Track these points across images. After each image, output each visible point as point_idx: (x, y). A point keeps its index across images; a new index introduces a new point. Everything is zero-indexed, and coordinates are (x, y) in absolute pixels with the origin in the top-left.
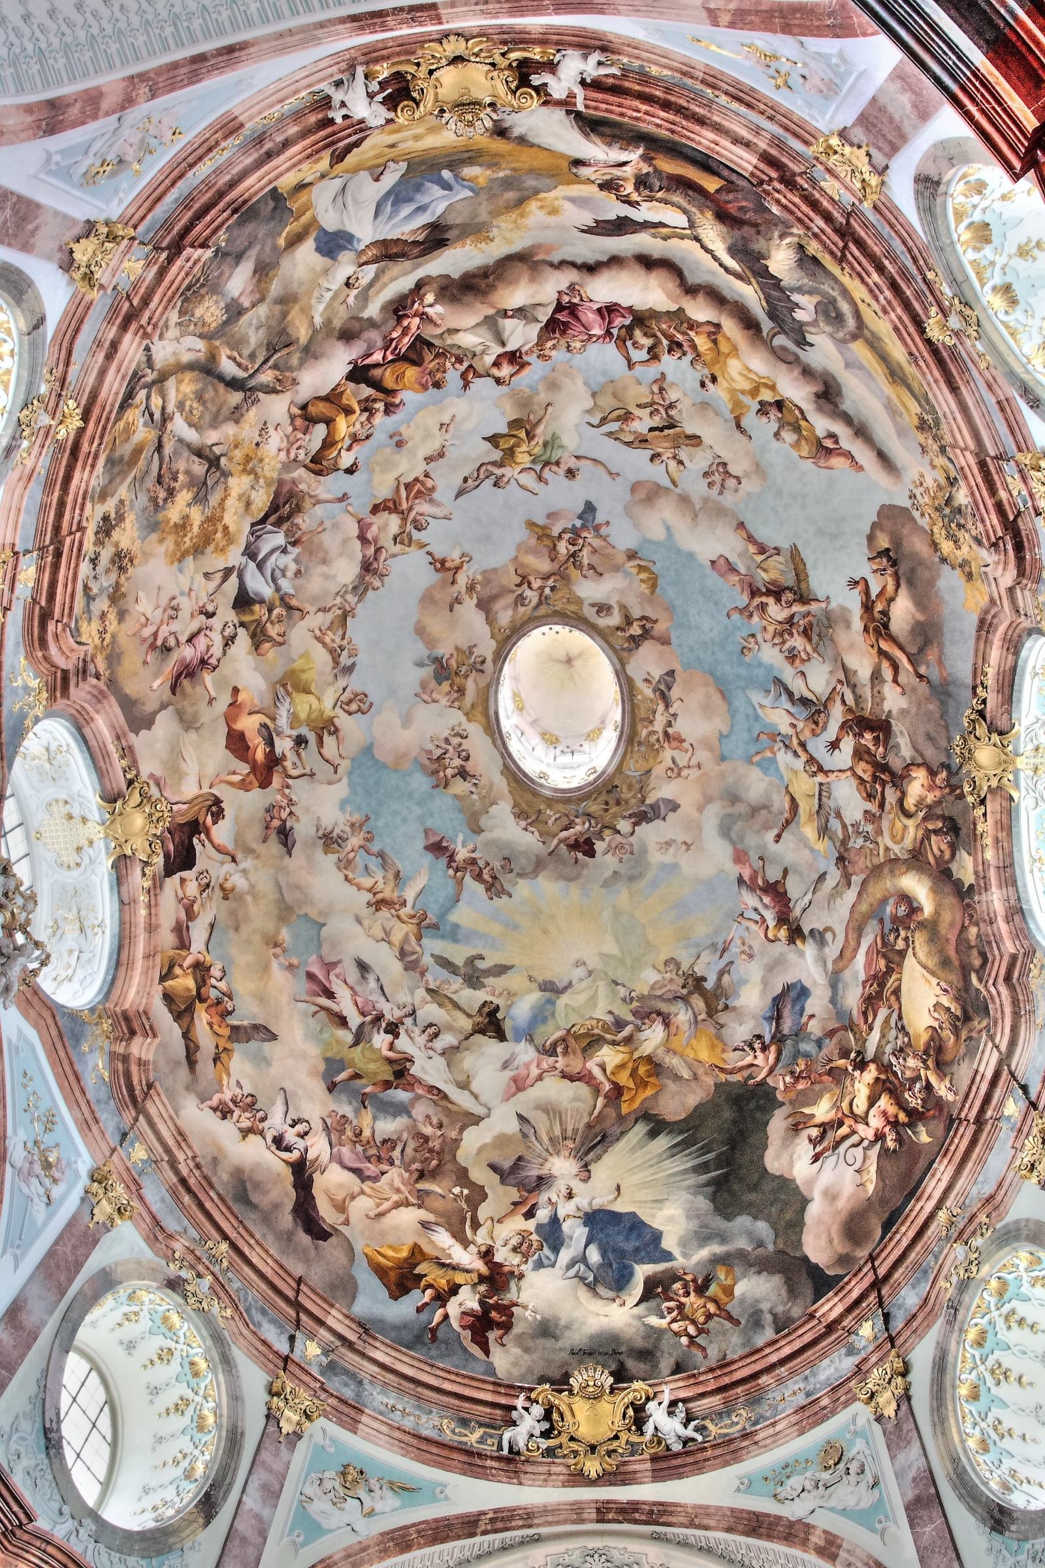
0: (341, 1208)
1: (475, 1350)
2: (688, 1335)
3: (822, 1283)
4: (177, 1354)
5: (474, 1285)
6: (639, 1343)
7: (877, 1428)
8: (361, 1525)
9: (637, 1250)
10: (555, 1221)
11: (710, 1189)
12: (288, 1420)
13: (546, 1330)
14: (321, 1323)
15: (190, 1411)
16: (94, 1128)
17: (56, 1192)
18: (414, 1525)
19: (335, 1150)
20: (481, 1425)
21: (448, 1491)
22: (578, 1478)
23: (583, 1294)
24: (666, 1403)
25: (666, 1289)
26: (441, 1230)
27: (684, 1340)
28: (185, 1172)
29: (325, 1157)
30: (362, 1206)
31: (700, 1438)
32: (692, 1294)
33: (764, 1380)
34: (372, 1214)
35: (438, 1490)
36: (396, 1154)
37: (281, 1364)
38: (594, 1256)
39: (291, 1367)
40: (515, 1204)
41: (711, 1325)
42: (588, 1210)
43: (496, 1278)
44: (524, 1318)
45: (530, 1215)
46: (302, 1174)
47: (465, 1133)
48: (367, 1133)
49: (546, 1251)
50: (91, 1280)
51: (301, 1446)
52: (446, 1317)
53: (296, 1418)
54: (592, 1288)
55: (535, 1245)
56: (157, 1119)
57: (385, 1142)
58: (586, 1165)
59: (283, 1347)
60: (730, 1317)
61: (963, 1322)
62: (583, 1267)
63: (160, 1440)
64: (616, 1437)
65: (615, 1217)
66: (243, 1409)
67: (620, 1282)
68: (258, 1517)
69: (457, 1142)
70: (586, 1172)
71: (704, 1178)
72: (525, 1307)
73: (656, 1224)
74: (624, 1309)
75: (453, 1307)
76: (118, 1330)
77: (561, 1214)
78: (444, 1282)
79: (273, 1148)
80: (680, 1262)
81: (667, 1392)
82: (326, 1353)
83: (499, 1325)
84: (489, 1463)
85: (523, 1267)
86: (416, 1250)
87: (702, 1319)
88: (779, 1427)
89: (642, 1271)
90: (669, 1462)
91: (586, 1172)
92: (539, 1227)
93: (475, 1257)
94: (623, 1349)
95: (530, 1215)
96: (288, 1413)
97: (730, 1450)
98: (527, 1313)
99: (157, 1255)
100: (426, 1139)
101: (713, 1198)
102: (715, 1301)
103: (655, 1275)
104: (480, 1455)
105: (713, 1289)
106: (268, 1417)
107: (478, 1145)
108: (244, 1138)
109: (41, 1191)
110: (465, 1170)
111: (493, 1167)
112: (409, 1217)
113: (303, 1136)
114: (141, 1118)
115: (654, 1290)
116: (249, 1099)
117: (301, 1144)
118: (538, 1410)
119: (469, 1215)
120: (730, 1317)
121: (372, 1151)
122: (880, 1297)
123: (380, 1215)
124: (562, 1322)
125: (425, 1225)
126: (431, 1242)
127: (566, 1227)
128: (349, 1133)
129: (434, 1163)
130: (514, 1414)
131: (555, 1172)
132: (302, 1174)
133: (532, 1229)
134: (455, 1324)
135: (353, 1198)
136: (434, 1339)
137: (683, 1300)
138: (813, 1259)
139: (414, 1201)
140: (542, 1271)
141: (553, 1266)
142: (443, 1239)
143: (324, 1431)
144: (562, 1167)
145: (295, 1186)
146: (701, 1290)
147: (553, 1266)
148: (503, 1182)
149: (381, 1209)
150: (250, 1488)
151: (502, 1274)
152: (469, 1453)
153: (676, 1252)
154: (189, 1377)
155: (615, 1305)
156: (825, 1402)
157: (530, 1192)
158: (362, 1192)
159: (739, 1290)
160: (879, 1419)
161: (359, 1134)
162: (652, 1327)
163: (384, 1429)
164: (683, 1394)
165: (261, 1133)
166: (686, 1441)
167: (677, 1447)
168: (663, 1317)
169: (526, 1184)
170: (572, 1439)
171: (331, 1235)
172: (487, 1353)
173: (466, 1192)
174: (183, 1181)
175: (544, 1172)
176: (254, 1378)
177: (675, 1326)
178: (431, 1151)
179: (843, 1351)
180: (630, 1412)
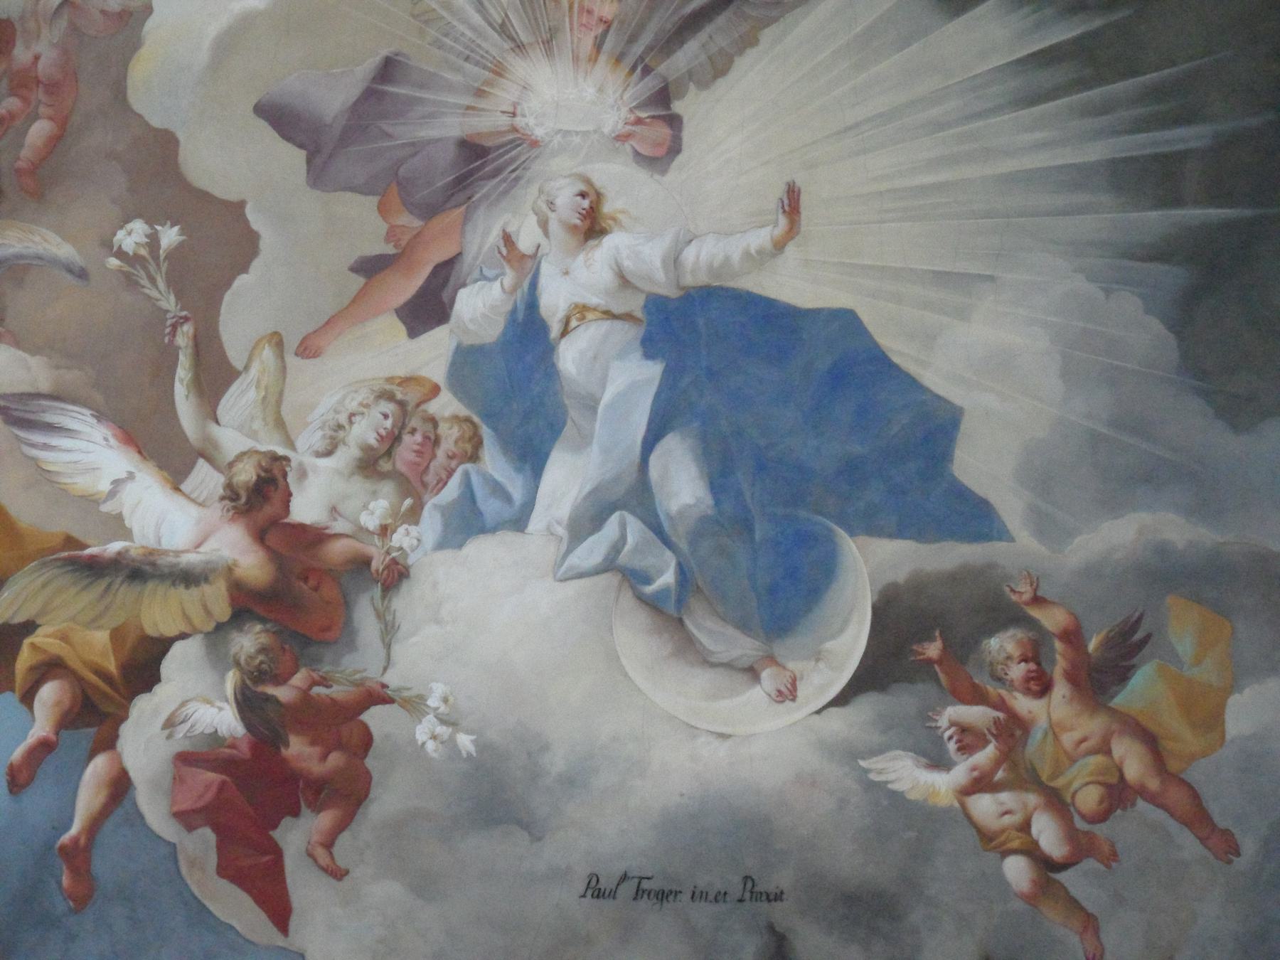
1: (235, 908)
2: (1032, 851)
6: (848, 862)
9: (852, 471)
10: (529, 333)
11: (1172, 277)
13: (497, 794)
23: (635, 641)
25: (962, 649)
26: (79, 420)
27: (1017, 870)
32: (1061, 689)
38: (682, 484)
40: (371, 268)
41: (1122, 830)
42: (663, 285)
43: (301, 594)
44: (415, 744)
45: (427, 310)
49: (494, 463)
52: (120, 786)
54: (668, 614)
55: (450, 435)
58: (663, 97)
60: (1197, 817)
62: (635, 530)
65: (773, 324)
67: (782, 601)
70: (660, 128)
71: (1155, 221)
72: (415, 706)
73: (934, 379)
75: (144, 742)
77: (555, 298)
78: (101, 637)
80: (1020, 548)
83: (319, 792)
85: (402, 538)
87: (1089, 798)
89: (869, 565)
91: (660, 128)
92: (467, 360)
93: (216, 512)
94: (783, 879)
95: (427, 310)
101: (1183, 315)
102: (1150, 740)
103: (919, 584)
105: (1143, 688)
107: (213, 30)
110: (167, 142)
111: (282, 118)
115: (912, 648)
119: (183, 338)
120: (1197, 817)
124: (556, 762)
126: (43, 477)
127: (570, 357)
129: (39, 131)
131: (535, 123)
133: (437, 372)
134: (153, 808)
136: (82, 897)
137: (1023, 704)
141: (519, 523)
142: (91, 455)
144: (566, 101)
146: (1099, 678)
147: (519, 523)
151: (317, 574)
153: (1011, 507)
155: (757, 695)
157: (429, 211)
159: (1244, 713)
162: (897, 798)
168: (939, 762)
169: (415, 172)
172: (279, 911)
173: (170, 236)
175: (488, 122)
177: (985, 806)
178: (23, 82)
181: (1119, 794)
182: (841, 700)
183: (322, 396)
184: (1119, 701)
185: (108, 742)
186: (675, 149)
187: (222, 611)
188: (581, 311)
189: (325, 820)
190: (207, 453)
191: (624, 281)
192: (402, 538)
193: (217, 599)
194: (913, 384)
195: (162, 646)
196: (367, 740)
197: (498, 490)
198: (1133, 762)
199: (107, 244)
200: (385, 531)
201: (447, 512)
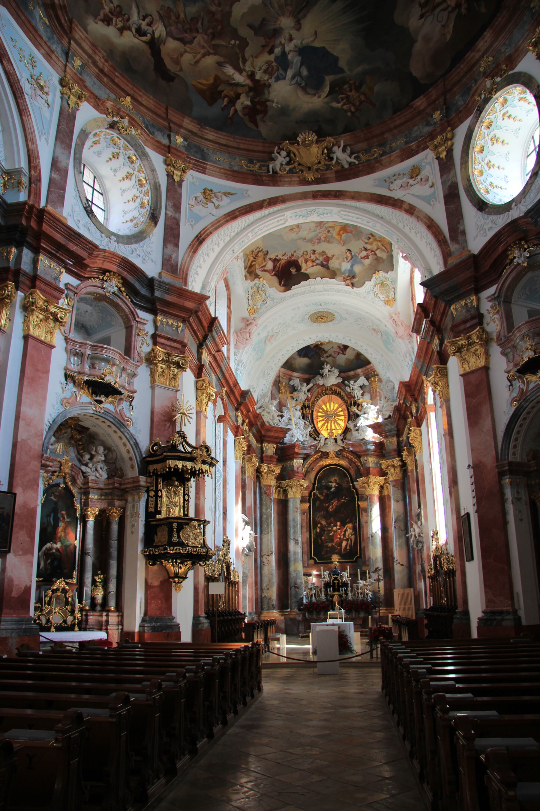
0: (177, 62)
1: (251, 125)
2: (351, 111)
3: (418, 89)
4: (121, 155)
5: (247, 94)
7: (436, 162)
8: (215, 211)
12: (177, 175)
13: (284, 111)
14: (181, 127)
15: (133, 178)
16: (53, 56)
17: (50, 98)
18: (236, 209)
19: (168, 29)
20: (259, 161)
21: (249, 193)
22: (304, 182)
23: (300, 93)
24: (342, 147)
26: (228, 66)
27: (349, 114)
28: (101, 65)
29: (164, 34)
30: (187, 58)
31: (357, 162)
32: (353, 91)
33: (386, 135)
34: (192, 63)
35: (244, 193)
36: (199, 25)
37: (167, 149)
38: (305, 72)
39: (172, 150)
40: (263, 46)
45: (271, 52)
46: (154, 45)
47: (234, 7)
48: (182, 16)
49: (281, 71)
50: (79, 137)
51: (184, 184)
52: (236, 111)
53: (179, 173)
56: (80, 41)
57: (192, 19)
59: (165, 142)
61: (483, 118)
63: (124, 191)
64: (319, 163)
66: (157, 174)
68: (174, 218)
69: (230, 13)
70: (298, 26)
72: (273, 102)
73: (335, 54)
74: (320, 99)
75: (239, 106)
76: (92, 148)
77: (287, 49)
78: (232, 93)
79: (137, 36)
81: (342, 142)
82: (185, 140)
84: (264, 178)
85: (270, 81)
86: (217, 78)
87: (358, 103)
88: (392, 158)
89: (328, 79)
90: (344, 174)
92: (276, 58)
95: (271, 52)
96: (176, 172)
97: (369, 168)
98: (274, 105)
99: (101, 113)
100: (213, 14)
102: (365, 95)
104: (260, 175)
105: (364, 88)
106: (167, 175)
107: (241, 14)
108: (121, 33)
109: (43, 101)
111: (250, 26)
112: (210, 61)
113: (150, 25)
114: (72, 42)
116: (118, 9)
117: (150, 30)
118: (284, 153)
119: (240, 55)
121: (187, 26)
122: (445, 100)
123: (197, 62)
125: (220, 64)
126: (224, 73)
127: (289, 57)
128: (173, 18)
129: (219, 27)
130: (273, 155)
132: (154, 45)
133: (273, 60)
134: (240, 114)
135: (182, 55)
137: (349, 93)
138: (415, 74)
139: (211, 51)
140: (280, 82)
141: (284, 78)
142: (230, 70)
143: (192, 176)
145: (153, 55)
147: (284, 78)
148: (256, 34)
149: (197, 58)
150: (168, 208)
152: (255, 175)
153: (346, 68)
154: (129, 163)
156: (414, 147)
158: (186, 51)
159: (376, 89)
160: (438, 158)
161: (178, 17)
163: (217, 169)
164: (349, 143)
165: (129, 29)
166: (350, 164)
167: (346, 166)
168: (339, 103)
169: (268, 34)
170: (300, 164)
171: (174, 78)
172: (257, 126)
173: (237, 42)
174: (101, 71)
176: (157, 159)
177: (345, 107)
179: (425, 123)
180: (326, 151)
181: (361, 102)
182: (326, 97)
183: (259, 63)
184: (361, 91)
185: (234, 105)
186: (300, 28)
187: (248, 90)
188: (290, 51)
189: (262, 116)
190: (245, 70)
191: (295, 46)
192: (270, 81)
193: (247, 89)
194: (332, 55)
195: (240, 94)
196: (267, 106)
197: (282, 75)
198: (363, 98)
199: (229, 43)
200: (268, 80)
201: (275, 78)
